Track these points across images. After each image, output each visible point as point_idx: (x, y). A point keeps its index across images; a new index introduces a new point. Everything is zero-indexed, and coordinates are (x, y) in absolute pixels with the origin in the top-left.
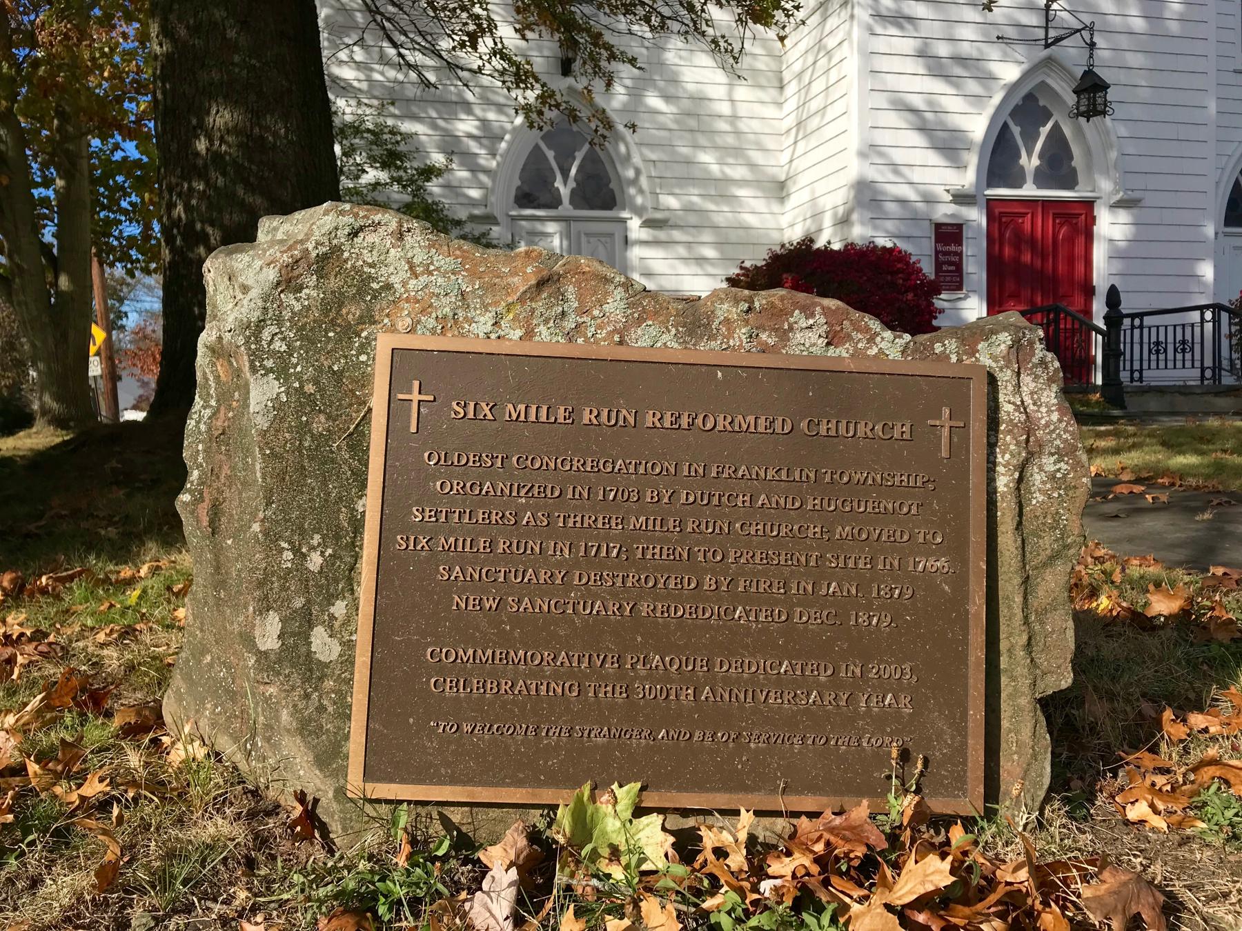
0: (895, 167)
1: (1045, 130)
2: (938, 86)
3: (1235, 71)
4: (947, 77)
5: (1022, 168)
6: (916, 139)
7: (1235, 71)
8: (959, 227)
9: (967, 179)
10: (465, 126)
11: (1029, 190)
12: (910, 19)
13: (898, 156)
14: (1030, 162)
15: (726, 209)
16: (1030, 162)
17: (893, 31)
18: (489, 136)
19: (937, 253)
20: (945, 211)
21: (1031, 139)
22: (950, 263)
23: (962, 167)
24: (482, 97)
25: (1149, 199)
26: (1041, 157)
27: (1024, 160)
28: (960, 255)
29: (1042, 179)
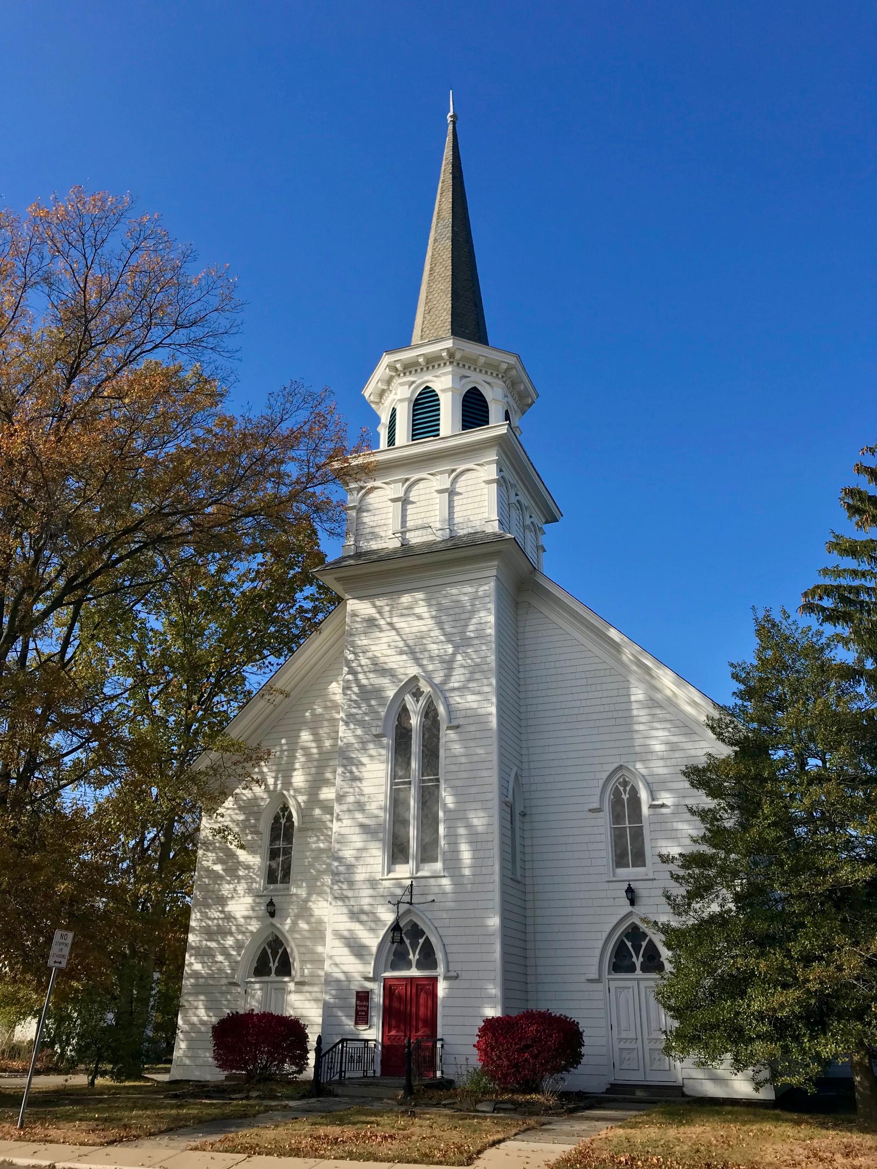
0: (336, 965)
1: (421, 941)
2: (356, 926)
3: (608, 882)
4: (361, 922)
5: (410, 961)
6: (346, 951)
7: (608, 882)
8: (368, 993)
9: (370, 970)
10: (230, 941)
11: (414, 972)
12: (347, 897)
13: (338, 960)
14: (414, 957)
15: (844, 873)
16: (414, 957)
17: (340, 903)
18: (239, 946)
19: (357, 1005)
20: (358, 984)
21: (414, 946)
22: (363, 1011)
23: (367, 963)
24: (237, 929)
25: (463, 975)
26: (419, 954)
27: (411, 956)
28: (368, 1007)
29: (420, 966)
